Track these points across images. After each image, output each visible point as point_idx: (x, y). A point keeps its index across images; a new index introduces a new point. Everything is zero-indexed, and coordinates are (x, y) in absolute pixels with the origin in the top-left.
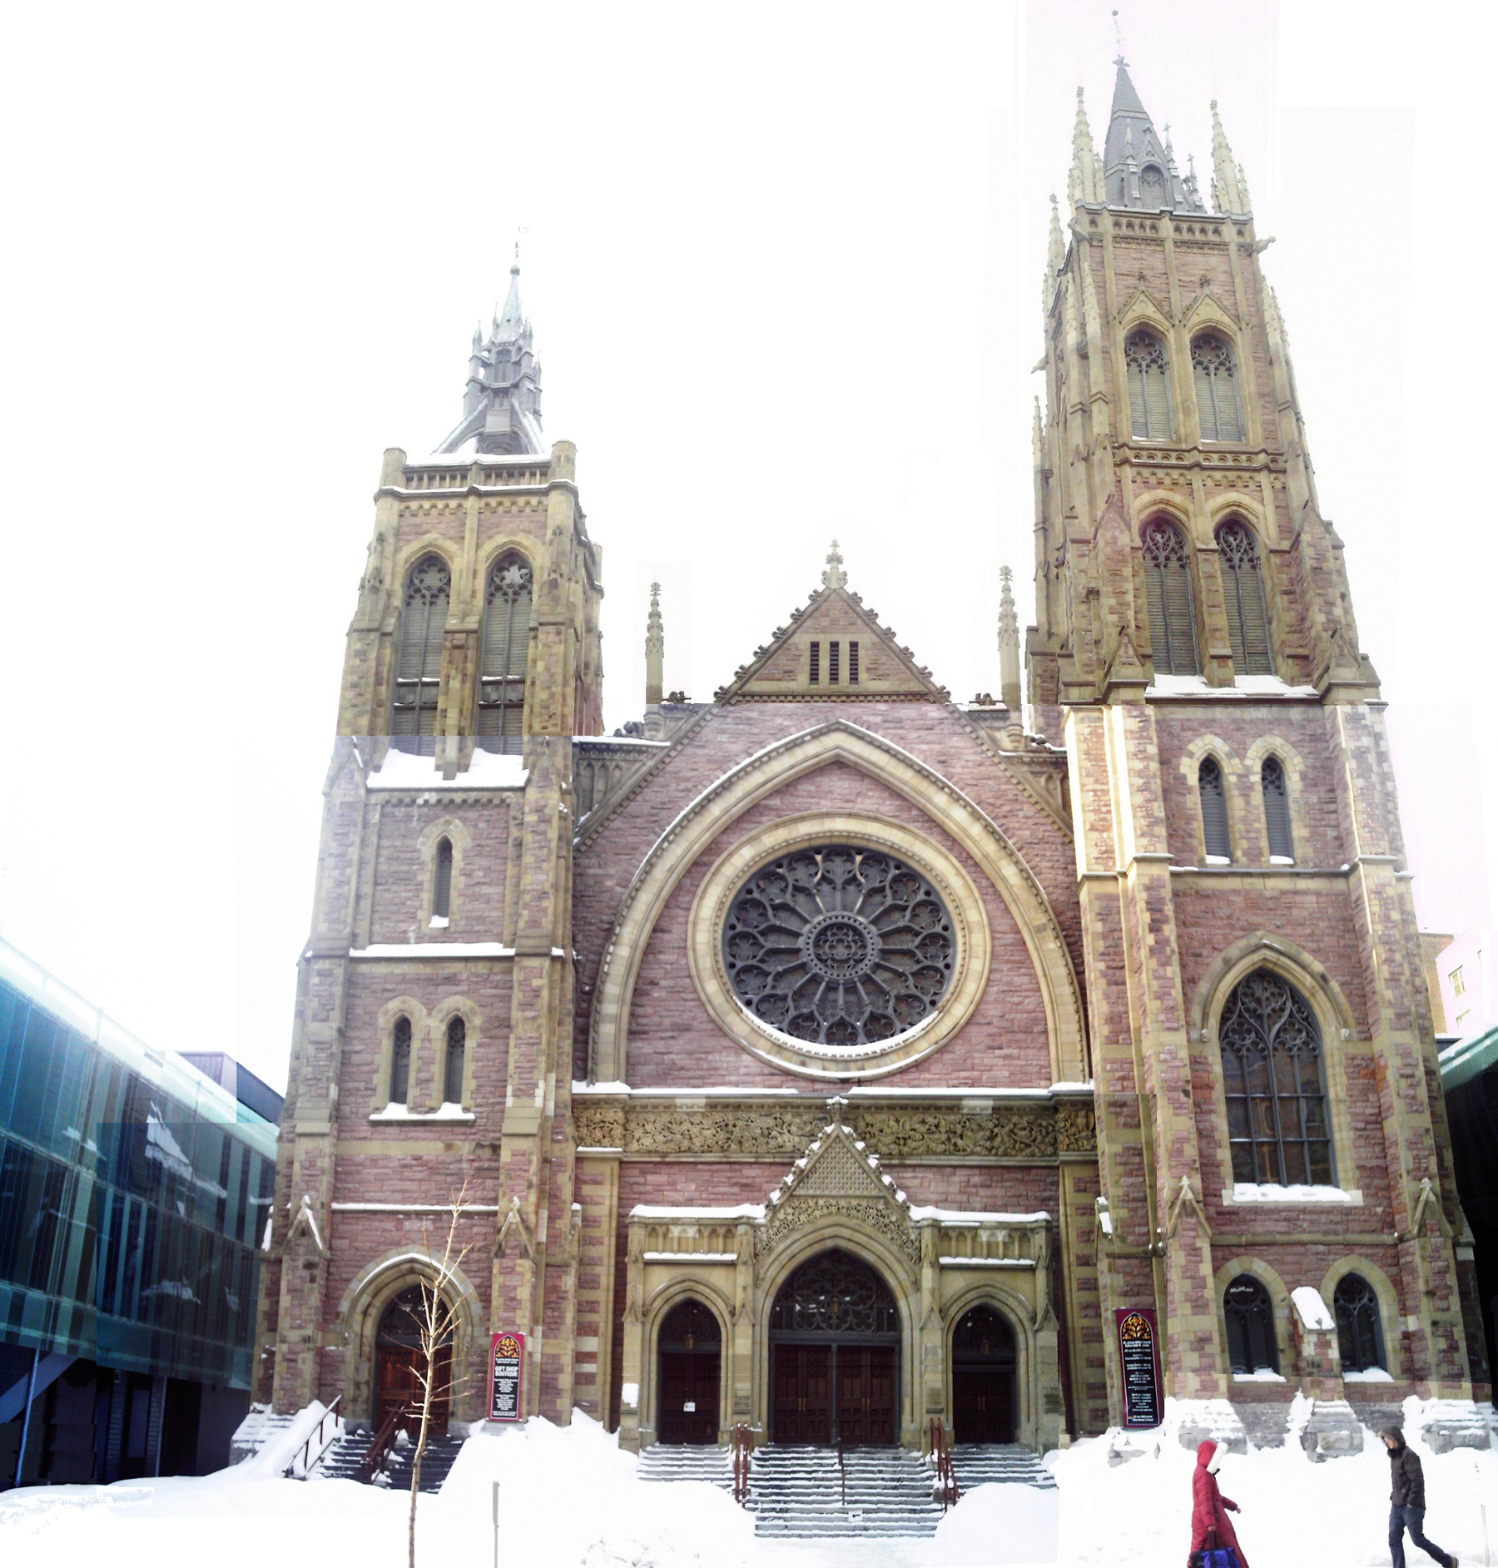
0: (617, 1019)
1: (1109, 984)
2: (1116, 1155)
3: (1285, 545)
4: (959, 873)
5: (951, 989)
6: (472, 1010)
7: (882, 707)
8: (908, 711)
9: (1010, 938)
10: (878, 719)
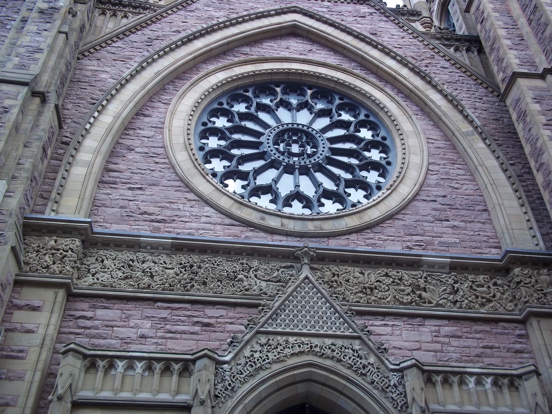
0: (90, 165)
4: (393, 99)
9: (441, 144)
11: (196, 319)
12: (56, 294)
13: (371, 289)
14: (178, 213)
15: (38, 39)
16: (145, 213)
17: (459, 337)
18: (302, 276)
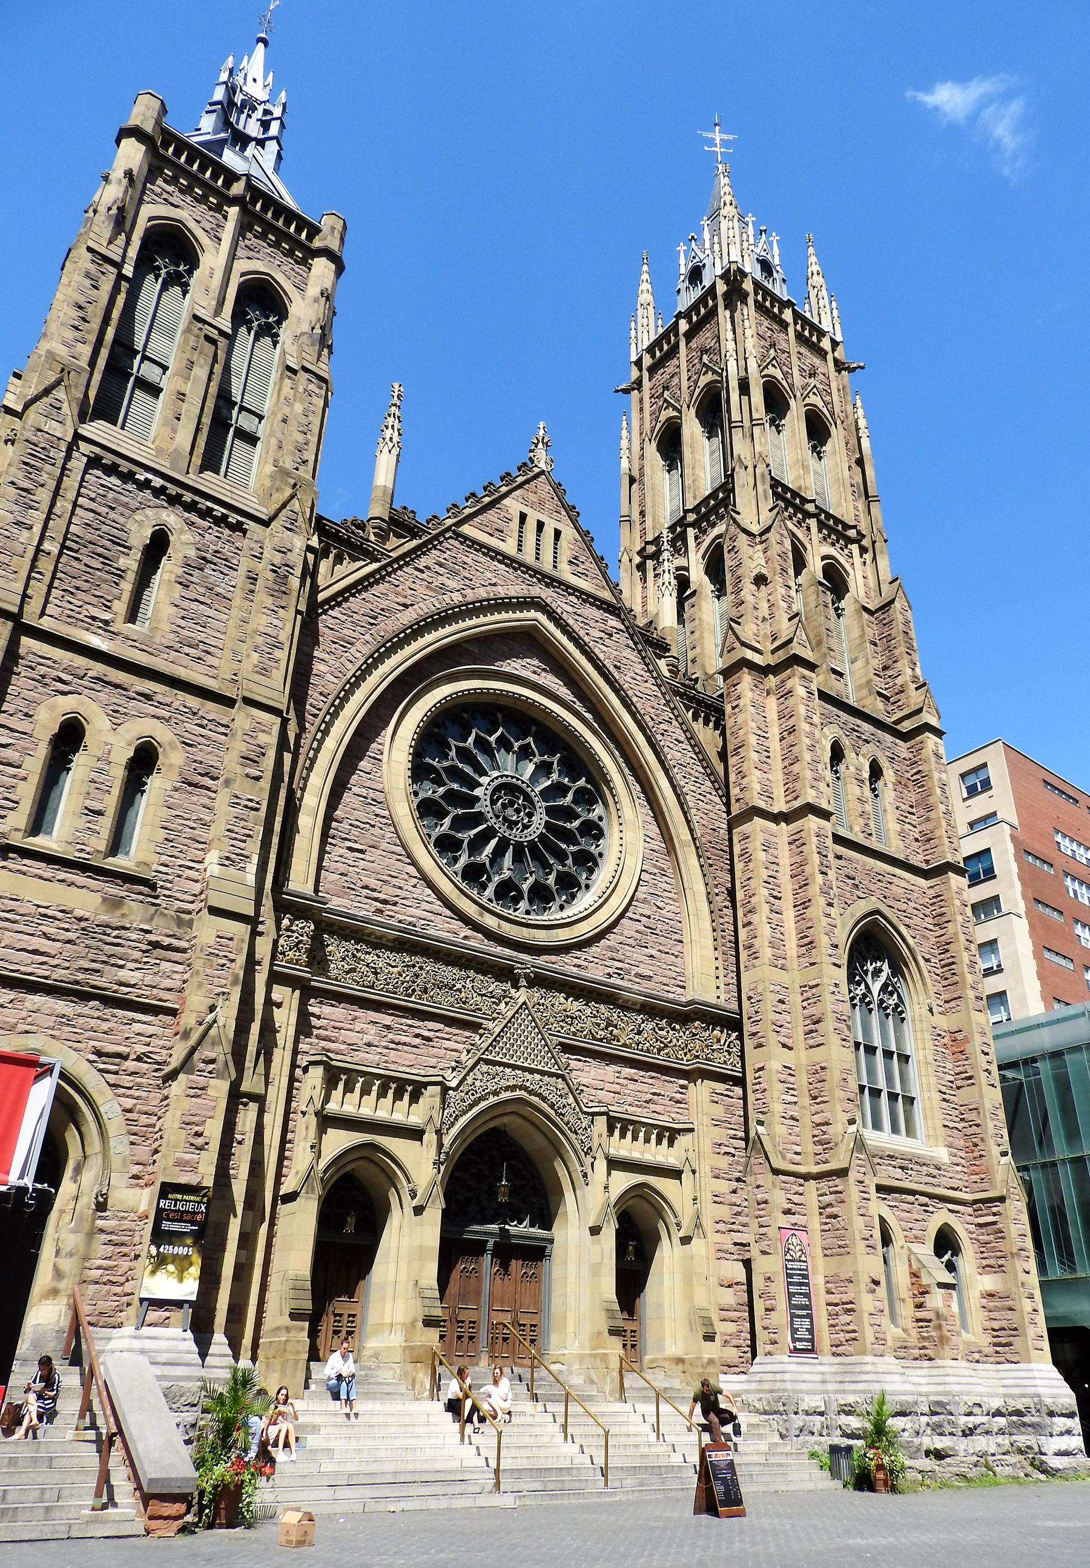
6: (171, 744)
7: (575, 601)
11: (417, 1031)
13: (572, 1018)
15: (276, 622)
16: (366, 887)
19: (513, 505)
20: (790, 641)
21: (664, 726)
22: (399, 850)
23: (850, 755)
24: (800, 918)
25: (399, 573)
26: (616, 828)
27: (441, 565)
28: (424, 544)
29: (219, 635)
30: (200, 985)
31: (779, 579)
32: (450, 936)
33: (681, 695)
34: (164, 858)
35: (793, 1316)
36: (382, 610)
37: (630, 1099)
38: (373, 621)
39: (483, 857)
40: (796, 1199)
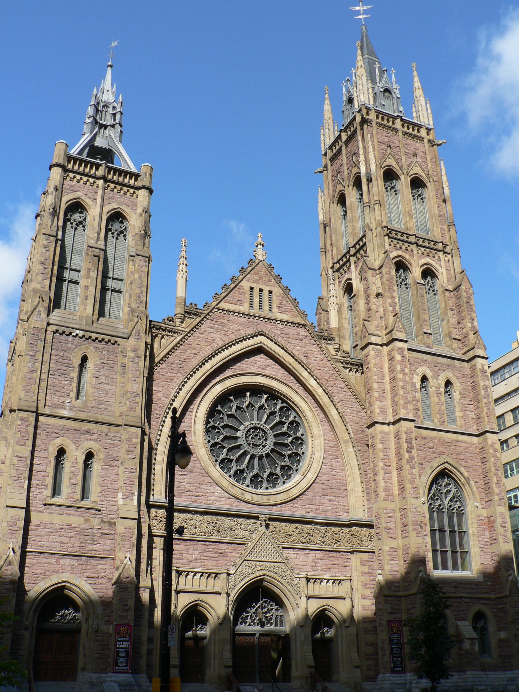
1: (385, 473)
2: (387, 551)
3: (451, 288)
5: (307, 465)
6: (99, 450)
7: (281, 326)
8: (292, 330)
10: (279, 332)
11: (216, 550)
12: (161, 540)
13: (290, 535)
14: (203, 490)
17: (323, 559)
18: (262, 532)
19: (246, 285)
20: (392, 330)
21: (333, 382)
22: (202, 471)
23: (432, 382)
24: (399, 475)
25: (192, 337)
26: (310, 440)
27: (211, 328)
28: (202, 320)
29: (113, 396)
30: (120, 548)
31: (387, 294)
32: (228, 507)
33: (342, 363)
34: (102, 498)
35: (393, 657)
36: (185, 359)
37: (320, 568)
38: (181, 366)
39: (244, 465)
40: (396, 607)
